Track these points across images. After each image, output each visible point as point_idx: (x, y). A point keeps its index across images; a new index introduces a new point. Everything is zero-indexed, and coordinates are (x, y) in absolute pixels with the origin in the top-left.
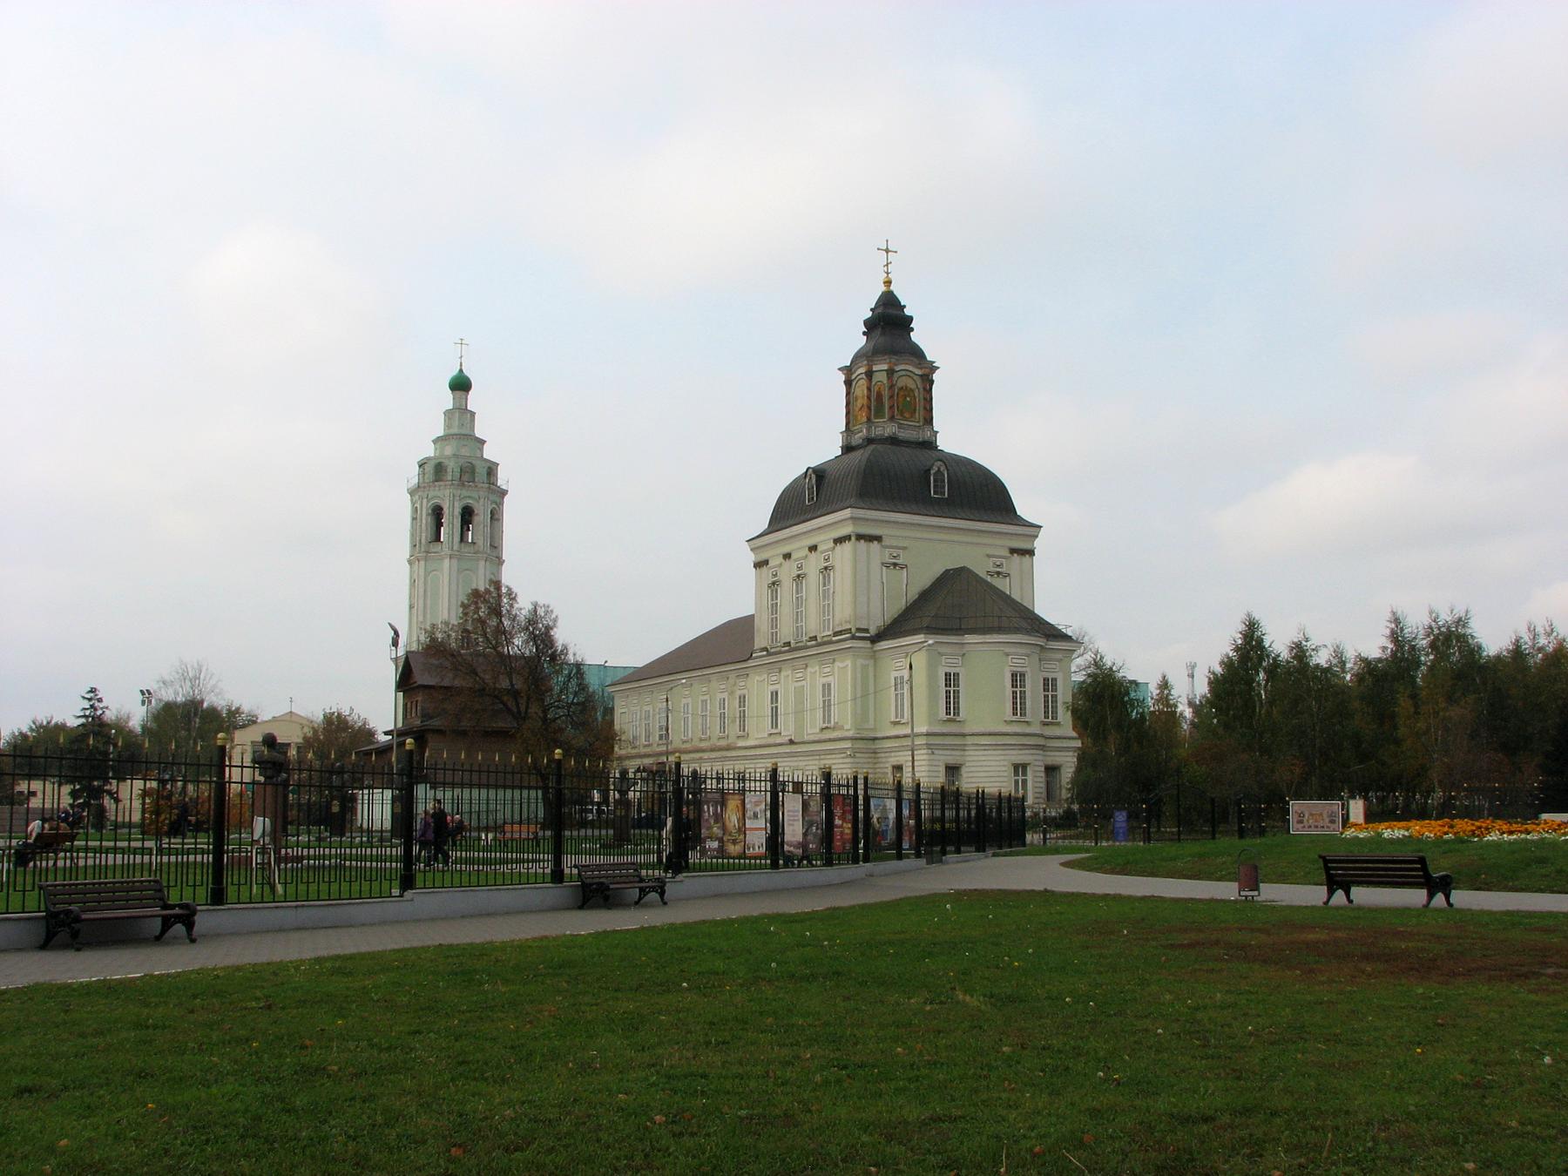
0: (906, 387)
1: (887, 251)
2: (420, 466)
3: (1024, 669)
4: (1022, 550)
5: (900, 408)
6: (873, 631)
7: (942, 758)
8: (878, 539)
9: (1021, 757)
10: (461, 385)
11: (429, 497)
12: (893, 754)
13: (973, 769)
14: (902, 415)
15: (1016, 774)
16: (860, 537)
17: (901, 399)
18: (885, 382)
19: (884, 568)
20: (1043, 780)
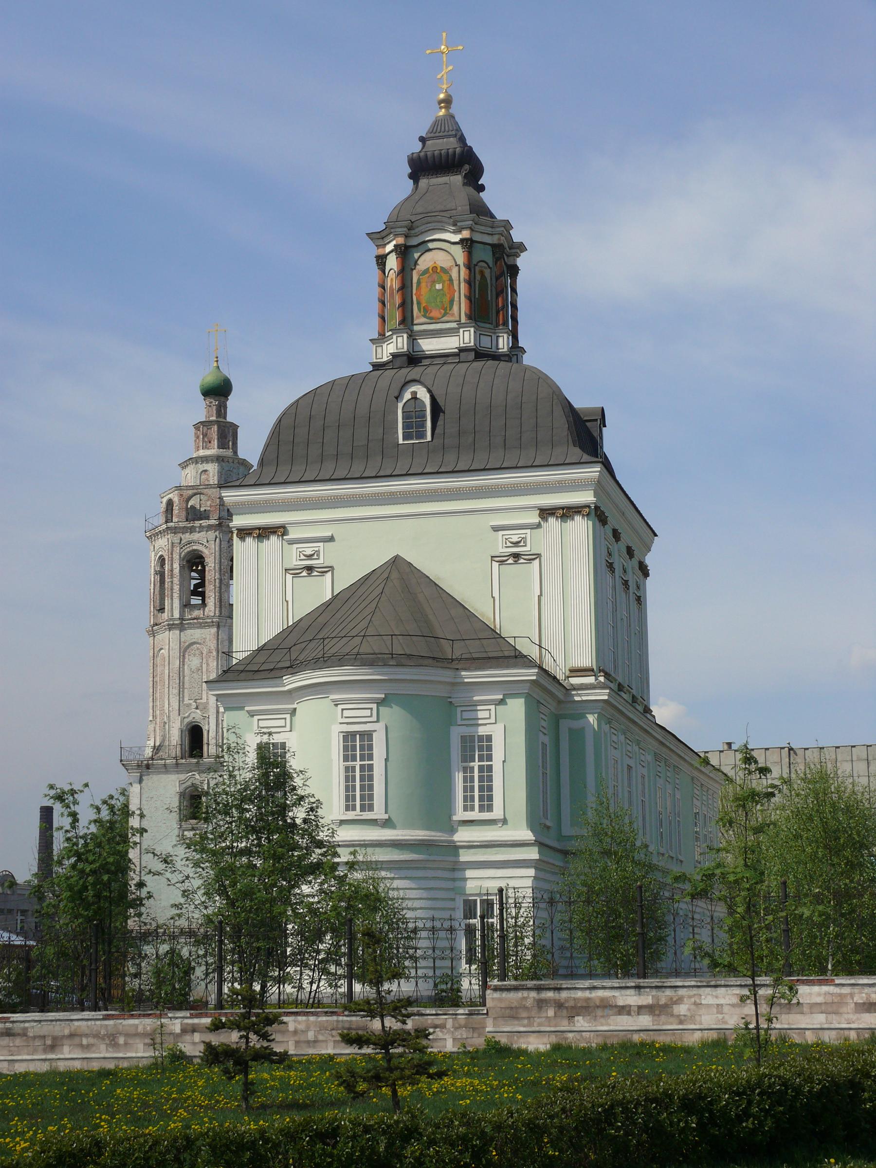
8: (280, 530)
14: (425, 316)
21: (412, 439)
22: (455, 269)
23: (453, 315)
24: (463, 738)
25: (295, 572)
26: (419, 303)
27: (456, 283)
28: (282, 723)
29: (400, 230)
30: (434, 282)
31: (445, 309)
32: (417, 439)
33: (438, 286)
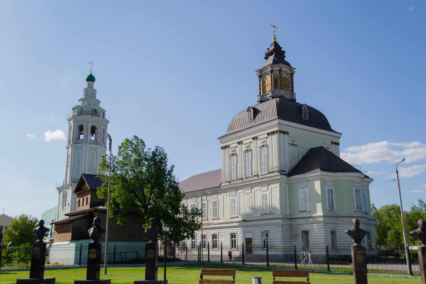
2: (73, 110)
4: (336, 143)
6: (287, 172)
8: (287, 133)
10: (91, 79)
11: (77, 121)
12: (302, 226)
16: (281, 132)
17: (284, 82)
18: (278, 74)
19: (290, 146)
21: (305, 118)
22: (289, 79)
23: (289, 90)
27: (289, 83)
30: (285, 81)
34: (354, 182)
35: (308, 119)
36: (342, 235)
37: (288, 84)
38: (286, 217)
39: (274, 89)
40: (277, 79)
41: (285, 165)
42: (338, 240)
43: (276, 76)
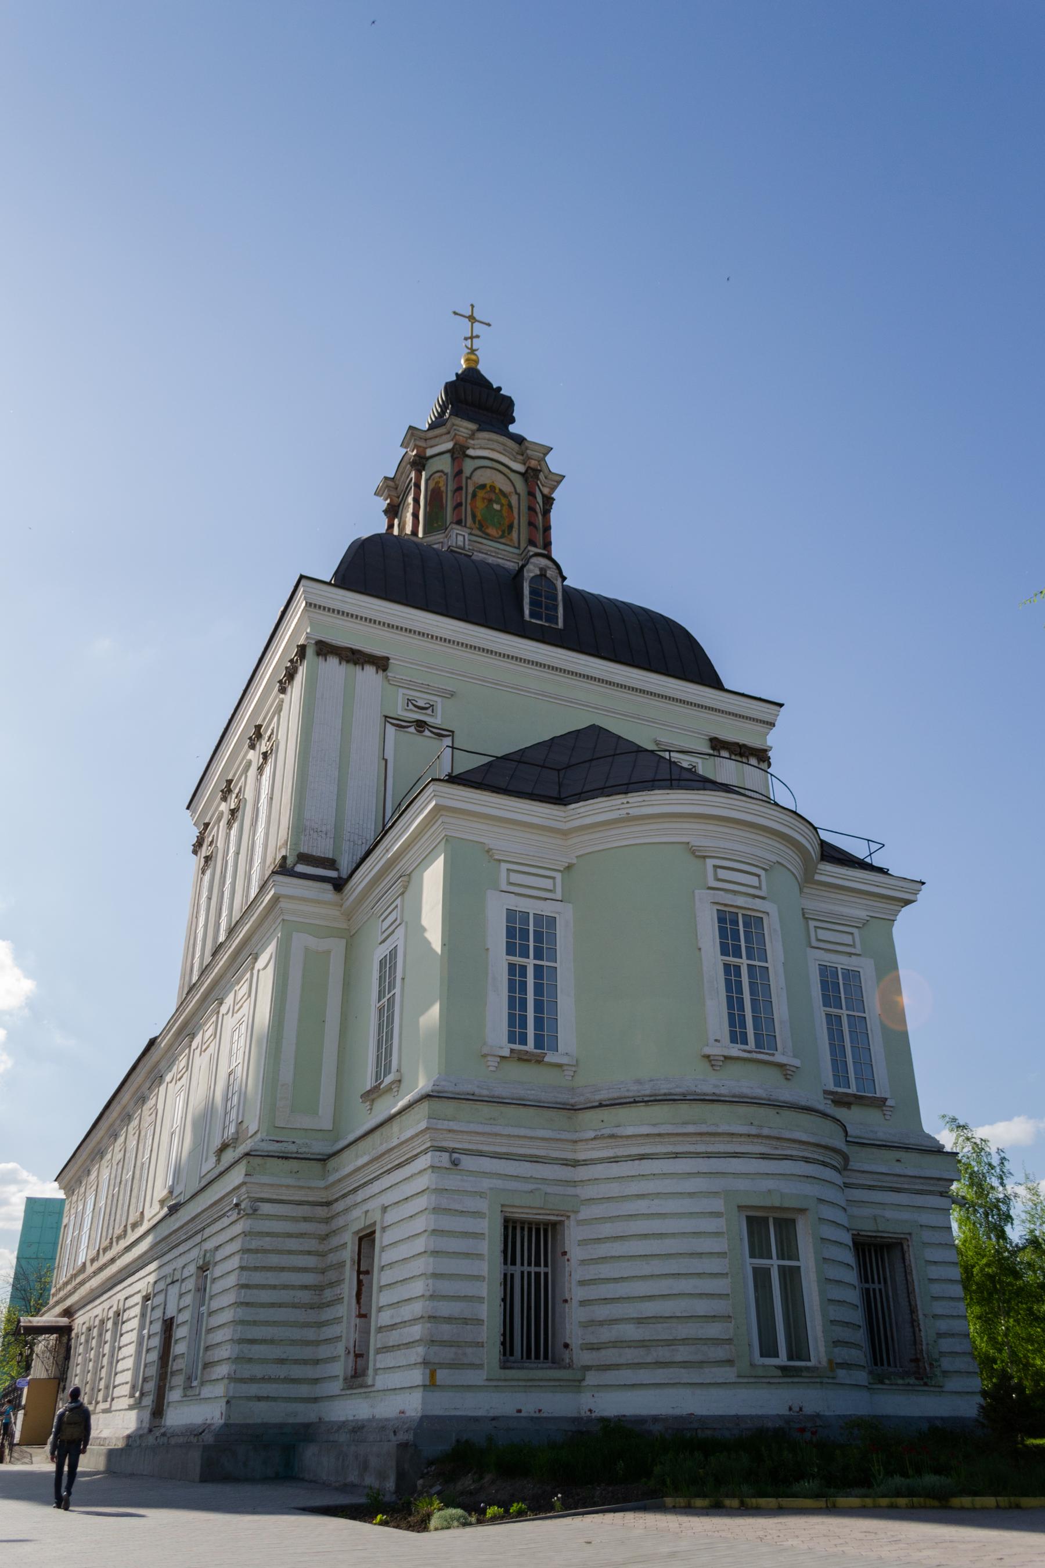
0: (493, 488)
1: (472, 318)
3: (758, 904)
5: (479, 517)
7: (486, 1184)
8: (381, 663)
9: (770, 1184)
13: (607, 1230)
15: (758, 1247)
17: (480, 505)
19: (391, 730)
20: (854, 1296)
21: (541, 619)
23: (511, 540)
24: (824, 969)
25: (400, 725)
26: (474, 516)
27: (515, 511)
28: (547, 884)
29: (464, 430)
30: (490, 501)
31: (503, 532)
32: (546, 621)
33: (496, 507)
34: (704, 857)
35: (561, 625)
36: (602, 1250)
37: (505, 513)
38: (293, 1148)
39: (425, 533)
40: (443, 489)
41: (338, 826)
42: (578, 1294)
43: (440, 477)
